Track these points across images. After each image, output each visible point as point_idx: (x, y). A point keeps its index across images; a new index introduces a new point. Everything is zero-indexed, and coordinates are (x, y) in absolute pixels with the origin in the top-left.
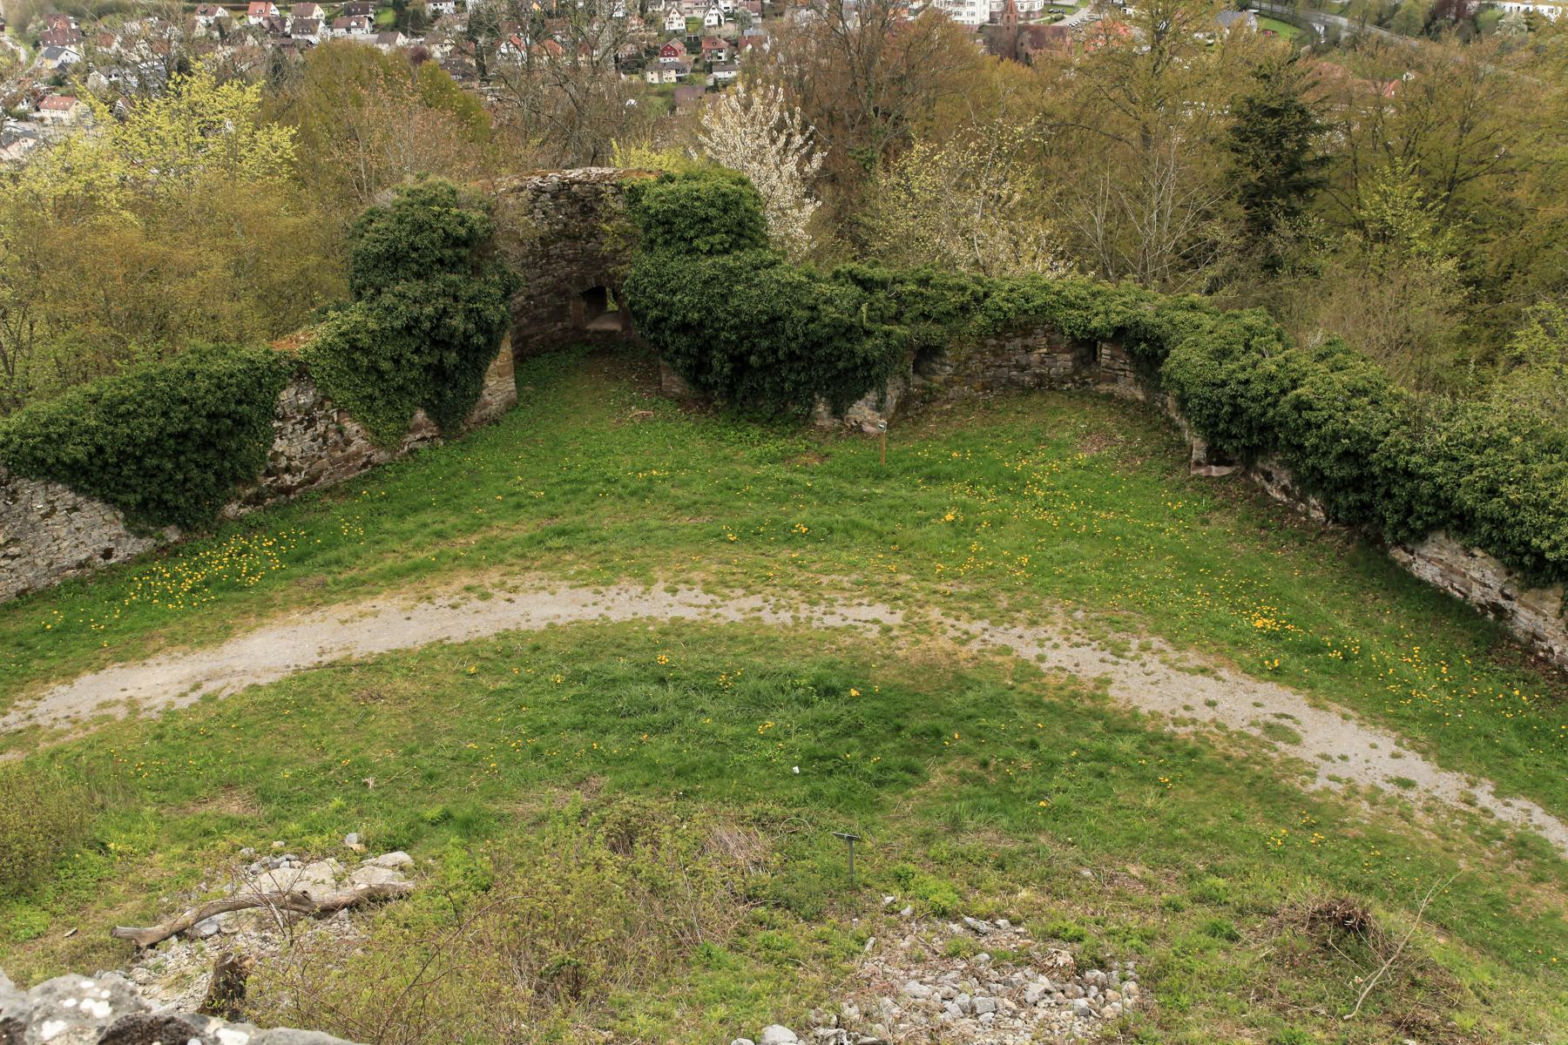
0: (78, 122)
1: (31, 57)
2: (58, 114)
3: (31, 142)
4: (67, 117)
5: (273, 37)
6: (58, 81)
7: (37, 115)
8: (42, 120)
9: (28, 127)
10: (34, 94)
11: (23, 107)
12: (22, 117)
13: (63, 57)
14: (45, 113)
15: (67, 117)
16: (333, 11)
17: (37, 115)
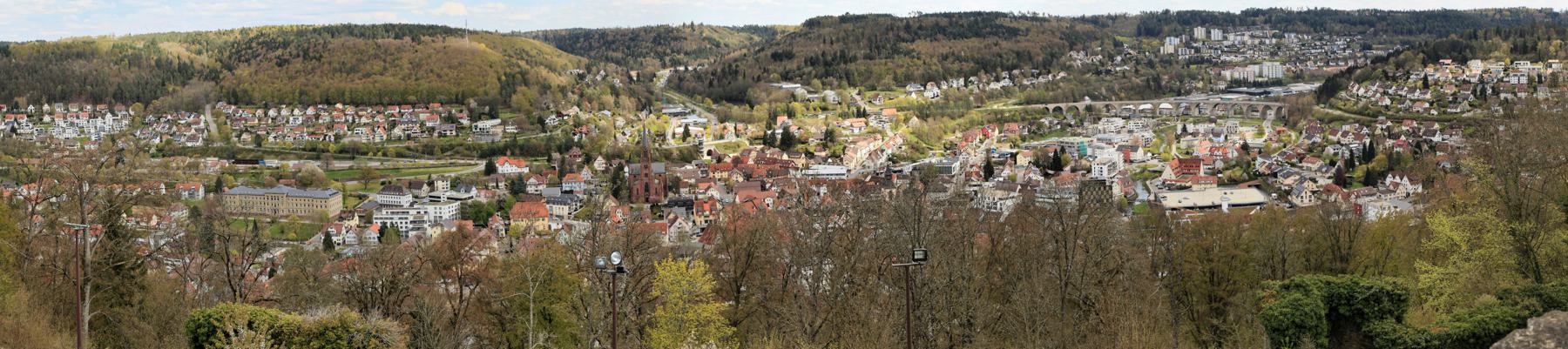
0: (1319, 170)
1: (1298, 138)
2: (1310, 165)
3: (1297, 177)
4: (1315, 167)
5: (1413, 137)
6: (1310, 150)
7: (1300, 165)
8: (1303, 167)
9: (1296, 170)
10: (1299, 154)
11: (1294, 160)
12: (1293, 165)
13: (1314, 139)
14: (1304, 164)
15: (1315, 167)
16: (1443, 127)
17: (1300, 165)
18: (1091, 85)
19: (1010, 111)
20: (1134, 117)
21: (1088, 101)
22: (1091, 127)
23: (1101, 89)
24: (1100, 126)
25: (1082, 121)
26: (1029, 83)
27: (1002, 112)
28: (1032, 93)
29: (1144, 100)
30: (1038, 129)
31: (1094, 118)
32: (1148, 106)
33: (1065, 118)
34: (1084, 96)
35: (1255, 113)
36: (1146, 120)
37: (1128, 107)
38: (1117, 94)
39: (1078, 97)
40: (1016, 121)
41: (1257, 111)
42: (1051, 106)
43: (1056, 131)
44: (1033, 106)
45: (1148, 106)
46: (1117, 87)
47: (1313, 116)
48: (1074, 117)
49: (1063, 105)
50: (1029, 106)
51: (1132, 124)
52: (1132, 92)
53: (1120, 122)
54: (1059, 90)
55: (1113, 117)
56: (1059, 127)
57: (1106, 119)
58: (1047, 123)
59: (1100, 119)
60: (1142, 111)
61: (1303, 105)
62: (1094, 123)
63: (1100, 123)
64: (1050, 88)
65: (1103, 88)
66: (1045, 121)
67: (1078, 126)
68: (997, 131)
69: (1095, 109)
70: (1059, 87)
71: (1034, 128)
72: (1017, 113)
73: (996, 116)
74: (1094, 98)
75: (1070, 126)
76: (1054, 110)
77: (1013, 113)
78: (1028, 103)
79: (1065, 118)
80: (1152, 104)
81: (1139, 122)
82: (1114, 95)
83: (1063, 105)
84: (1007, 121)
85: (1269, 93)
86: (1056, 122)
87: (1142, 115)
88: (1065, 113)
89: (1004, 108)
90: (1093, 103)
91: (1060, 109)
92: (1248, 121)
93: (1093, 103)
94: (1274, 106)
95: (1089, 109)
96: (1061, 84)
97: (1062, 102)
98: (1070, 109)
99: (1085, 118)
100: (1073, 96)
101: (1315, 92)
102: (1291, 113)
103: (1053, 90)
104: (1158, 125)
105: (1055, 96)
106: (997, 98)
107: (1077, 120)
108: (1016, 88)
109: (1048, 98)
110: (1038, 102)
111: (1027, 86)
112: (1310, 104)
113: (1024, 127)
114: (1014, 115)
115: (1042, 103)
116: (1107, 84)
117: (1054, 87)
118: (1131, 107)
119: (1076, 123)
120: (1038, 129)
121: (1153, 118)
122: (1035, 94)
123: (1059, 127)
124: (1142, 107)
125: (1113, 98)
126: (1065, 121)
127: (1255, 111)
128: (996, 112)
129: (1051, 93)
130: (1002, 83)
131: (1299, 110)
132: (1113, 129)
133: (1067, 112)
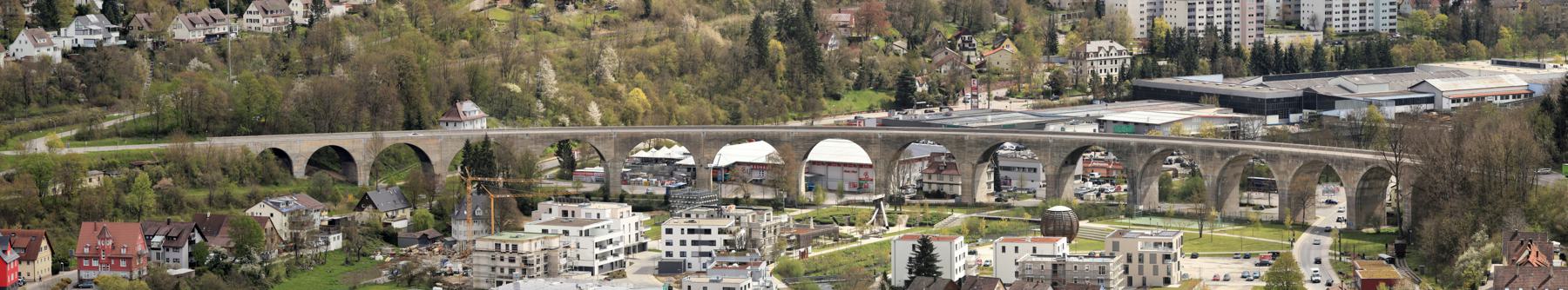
18: (486, 48)
19: (107, 167)
20: (690, 201)
21: (475, 122)
22: (485, 244)
23: (533, 65)
24: (532, 236)
25: (443, 217)
26: (200, 36)
27: (70, 171)
28: (212, 82)
29: (736, 119)
30: (241, 251)
31: (501, 204)
32: (758, 152)
33: (365, 201)
34: (456, 98)
35: (1258, 198)
36: (747, 215)
37: (663, 153)
38: (614, 95)
39: (427, 106)
40: (135, 213)
41: (1270, 187)
42: (301, 147)
43: (320, 260)
44: (219, 142)
45: (758, 152)
46: (610, 61)
47: (1530, 216)
48: (409, 198)
49: (355, 142)
50: (199, 144)
51: (676, 237)
52: (682, 86)
53: (621, 223)
54: (339, 70)
55: (589, 197)
56: (336, 242)
57: (557, 208)
58: (280, 221)
59: (527, 208)
60: (727, 174)
61: (1487, 163)
62: (502, 228)
63: (531, 227)
64: (297, 60)
65: (546, 65)
66: (273, 215)
67: (425, 240)
68: (44, 261)
69: (508, 157)
70: (342, 58)
71: (218, 245)
72: (142, 177)
73: (43, 188)
74: (502, 109)
75: (390, 237)
76: (318, 161)
77: (121, 175)
78: (194, 130)
79: (365, 201)
80: (773, 141)
81: (715, 224)
82: (598, 95)
83: (355, 142)
84: (89, 213)
85: (1329, 102)
86: (321, 218)
87: (728, 191)
88: (363, 178)
89: (80, 150)
90: (500, 131)
91: (341, 157)
92: (1227, 232)
93: (500, 131)
94: (1348, 162)
95: (478, 158)
96: (351, 42)
97: (355, 127)
98: (387, 161)
99: (461, 201)
100: (407, 97)
101: (1546, 104)
102: (1425, 198)
103: (310, 70)
104: (798, 242)
105: (320, 96)
106: (46, 101)
107: (423, 210)
108: (139, 57)
109: (289, 107)
110: (236, 125)
111: (189, 52)
112: (1521, 162)
113: (171, 242)
114: (127, 186)
115: (257, 130)
116: (564, 44)
117: (318, 55)
118: (677, 152)
119: (413, 227)
120: (241, 251)
121: (777, 206)
122: (225, 85)
123: (336, 242)
124: (727, 155)
125: (594, 111)
126: (365, 215)
127: (1259, 187)
128: (40, 173)
129: (301, 85)
130: (70, 36)
131: (1466, 187)
132: (588, 255)
133: (375, 173)
